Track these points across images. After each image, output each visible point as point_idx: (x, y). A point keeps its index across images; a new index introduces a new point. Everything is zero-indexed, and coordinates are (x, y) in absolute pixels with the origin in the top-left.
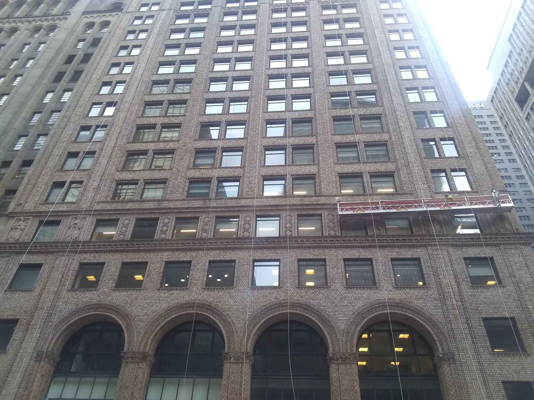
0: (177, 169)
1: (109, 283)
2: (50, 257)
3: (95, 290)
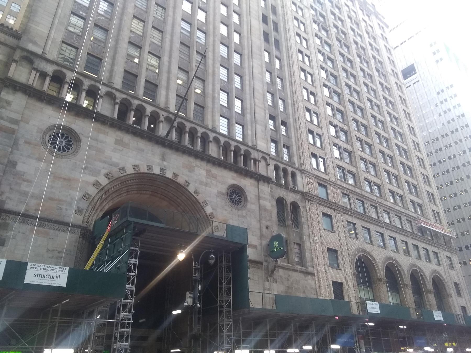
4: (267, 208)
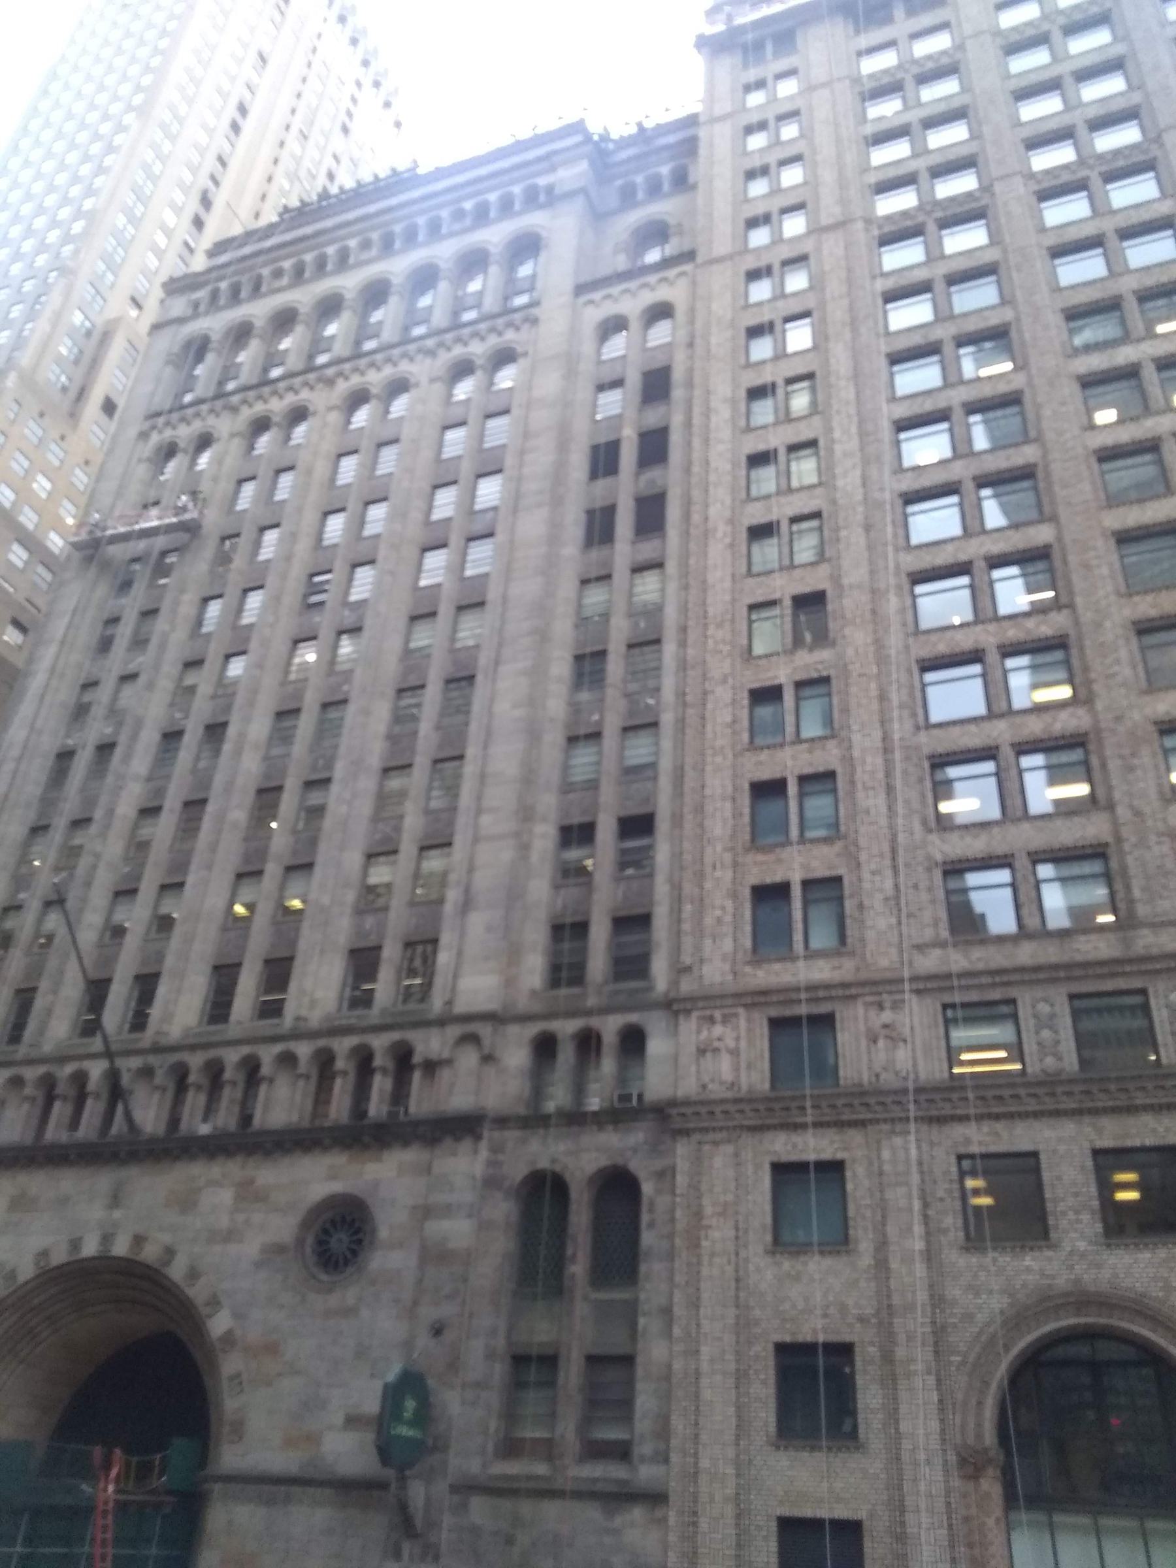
0: (1131, 807)
1: (1078, 1221)
2: (855, 1137)
3: (1049, 1247)
4: (451, 1245)
